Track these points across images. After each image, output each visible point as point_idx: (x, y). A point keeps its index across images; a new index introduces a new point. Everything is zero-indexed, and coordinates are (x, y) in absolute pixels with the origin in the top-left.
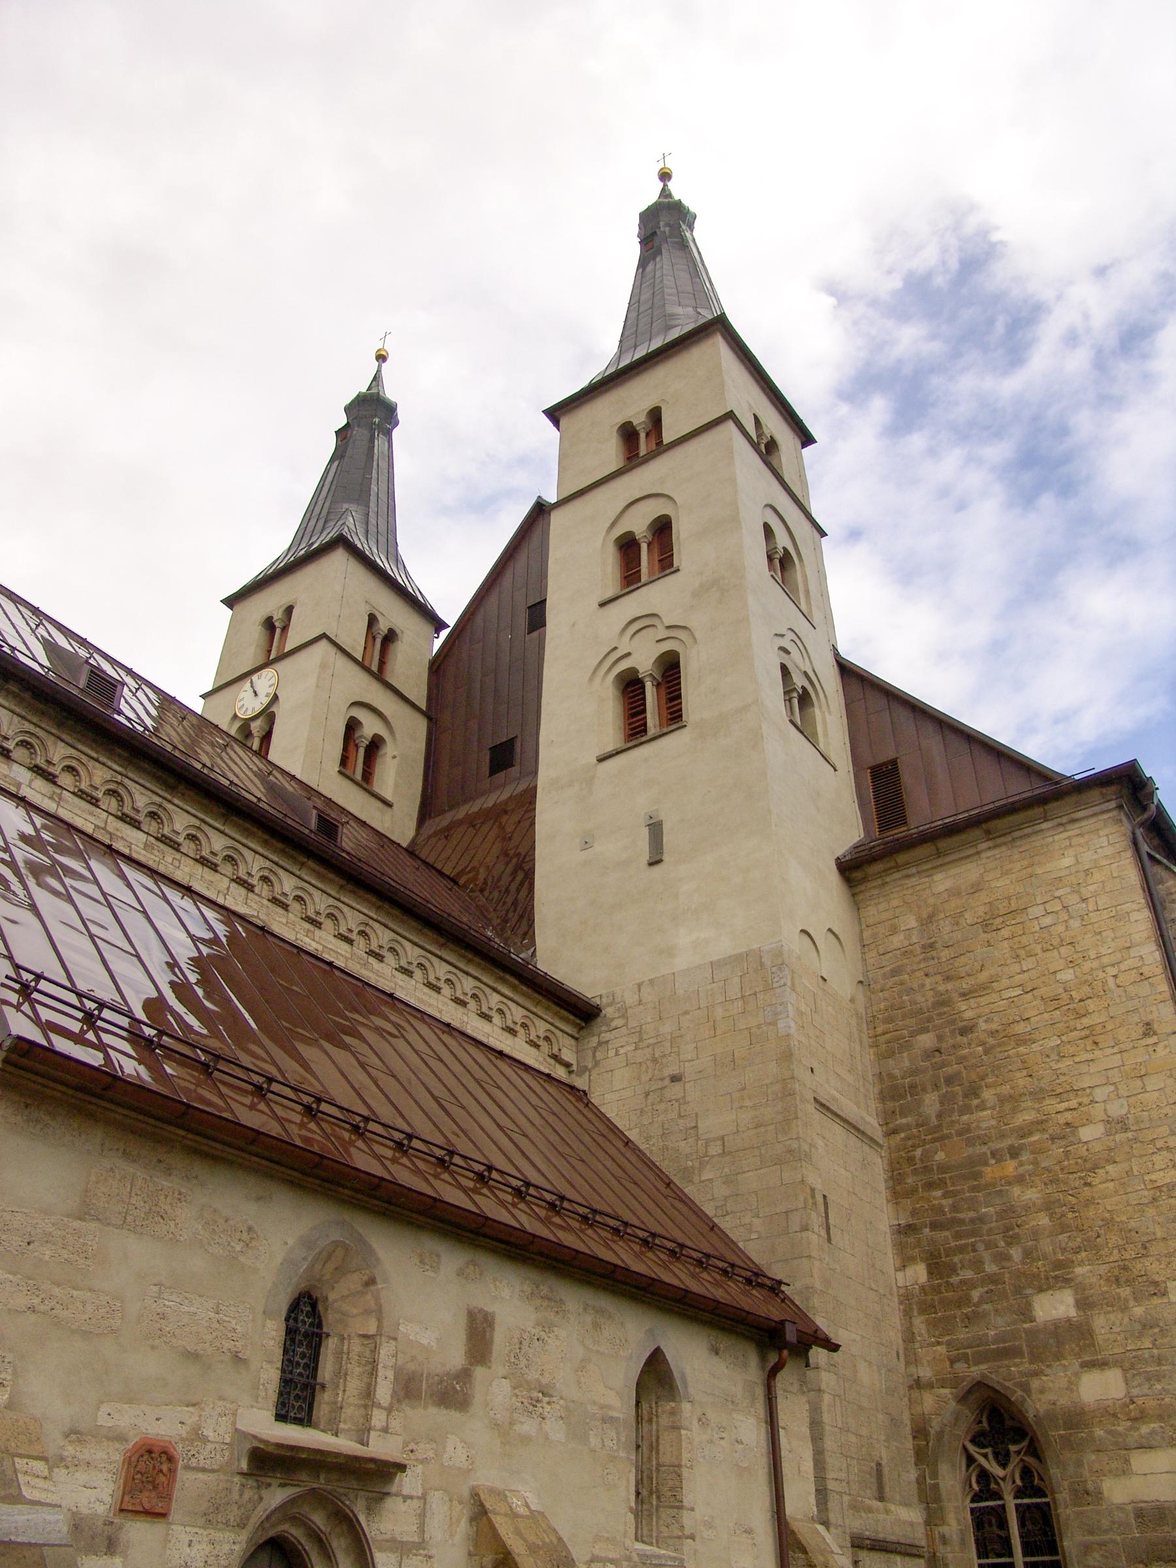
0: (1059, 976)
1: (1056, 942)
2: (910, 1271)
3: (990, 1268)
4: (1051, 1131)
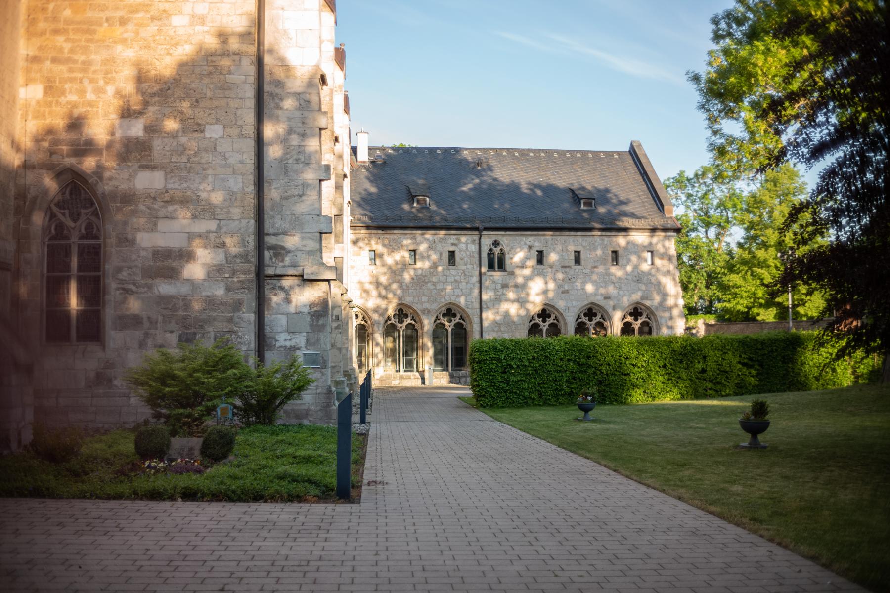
2: (31, 88)
4: (152, 13)
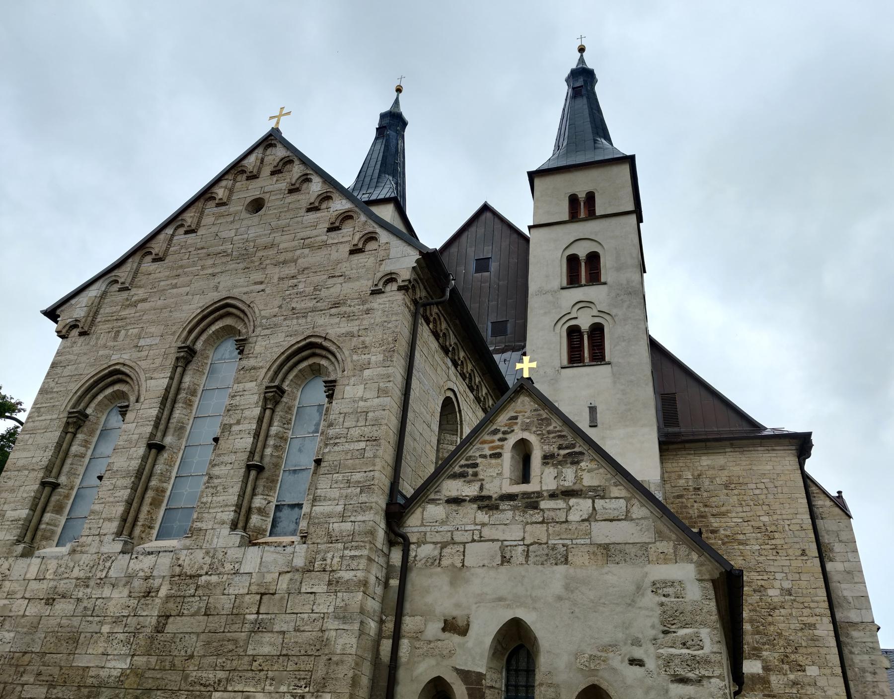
0: (761, 518)
1: (761, 502)
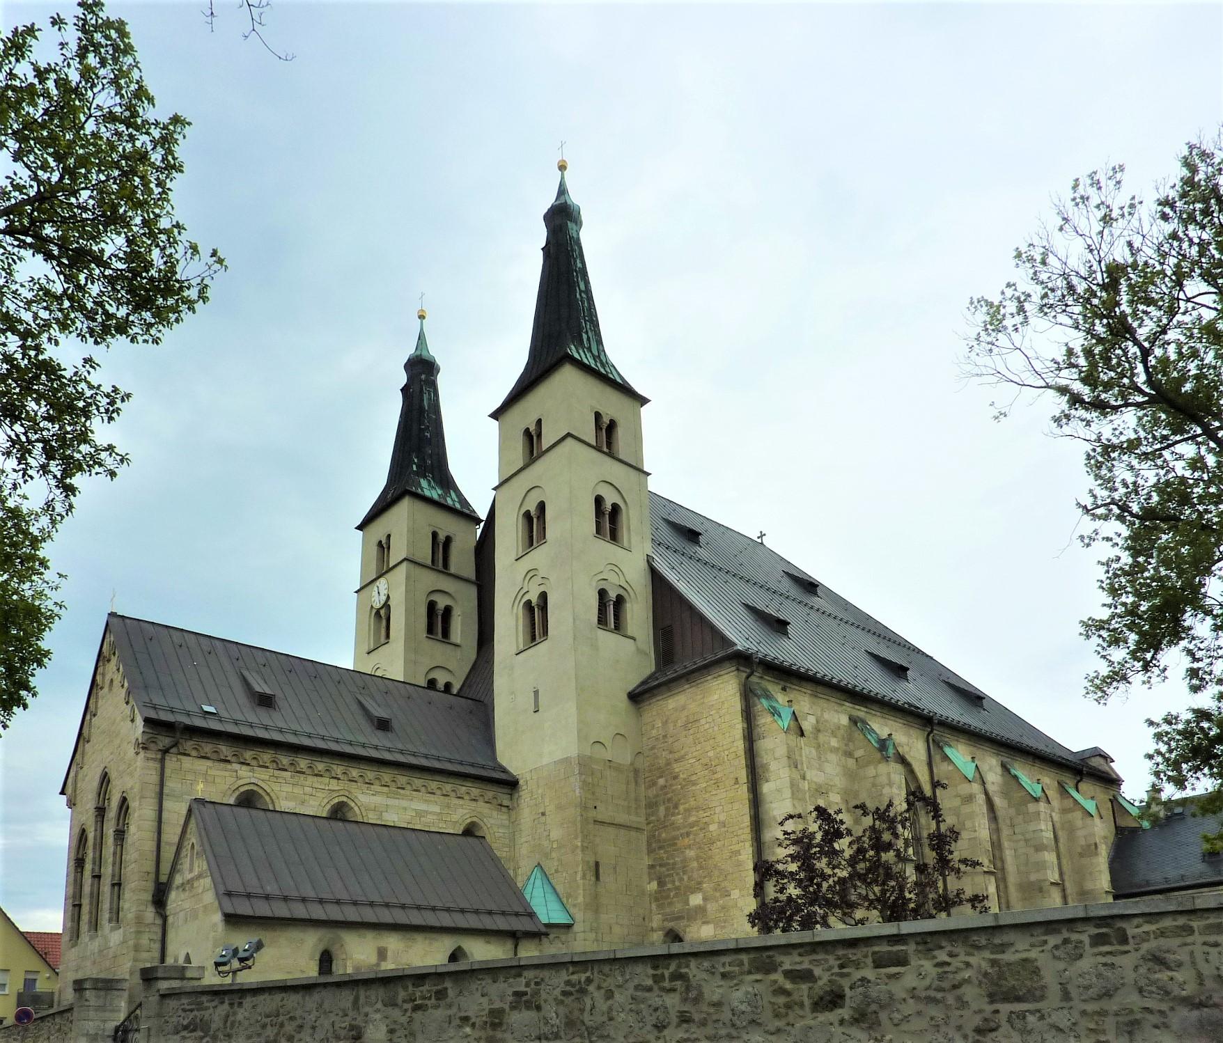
3: (677, 883)
